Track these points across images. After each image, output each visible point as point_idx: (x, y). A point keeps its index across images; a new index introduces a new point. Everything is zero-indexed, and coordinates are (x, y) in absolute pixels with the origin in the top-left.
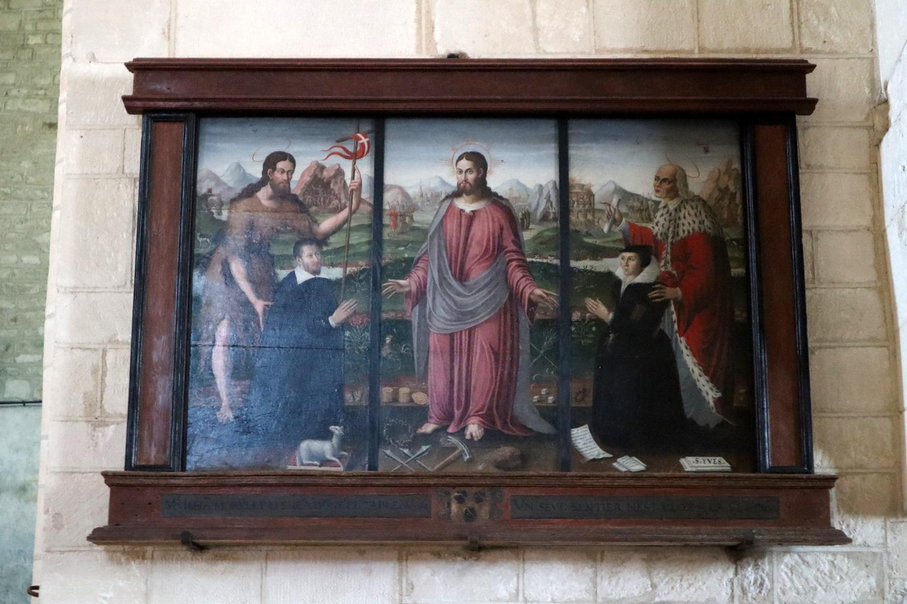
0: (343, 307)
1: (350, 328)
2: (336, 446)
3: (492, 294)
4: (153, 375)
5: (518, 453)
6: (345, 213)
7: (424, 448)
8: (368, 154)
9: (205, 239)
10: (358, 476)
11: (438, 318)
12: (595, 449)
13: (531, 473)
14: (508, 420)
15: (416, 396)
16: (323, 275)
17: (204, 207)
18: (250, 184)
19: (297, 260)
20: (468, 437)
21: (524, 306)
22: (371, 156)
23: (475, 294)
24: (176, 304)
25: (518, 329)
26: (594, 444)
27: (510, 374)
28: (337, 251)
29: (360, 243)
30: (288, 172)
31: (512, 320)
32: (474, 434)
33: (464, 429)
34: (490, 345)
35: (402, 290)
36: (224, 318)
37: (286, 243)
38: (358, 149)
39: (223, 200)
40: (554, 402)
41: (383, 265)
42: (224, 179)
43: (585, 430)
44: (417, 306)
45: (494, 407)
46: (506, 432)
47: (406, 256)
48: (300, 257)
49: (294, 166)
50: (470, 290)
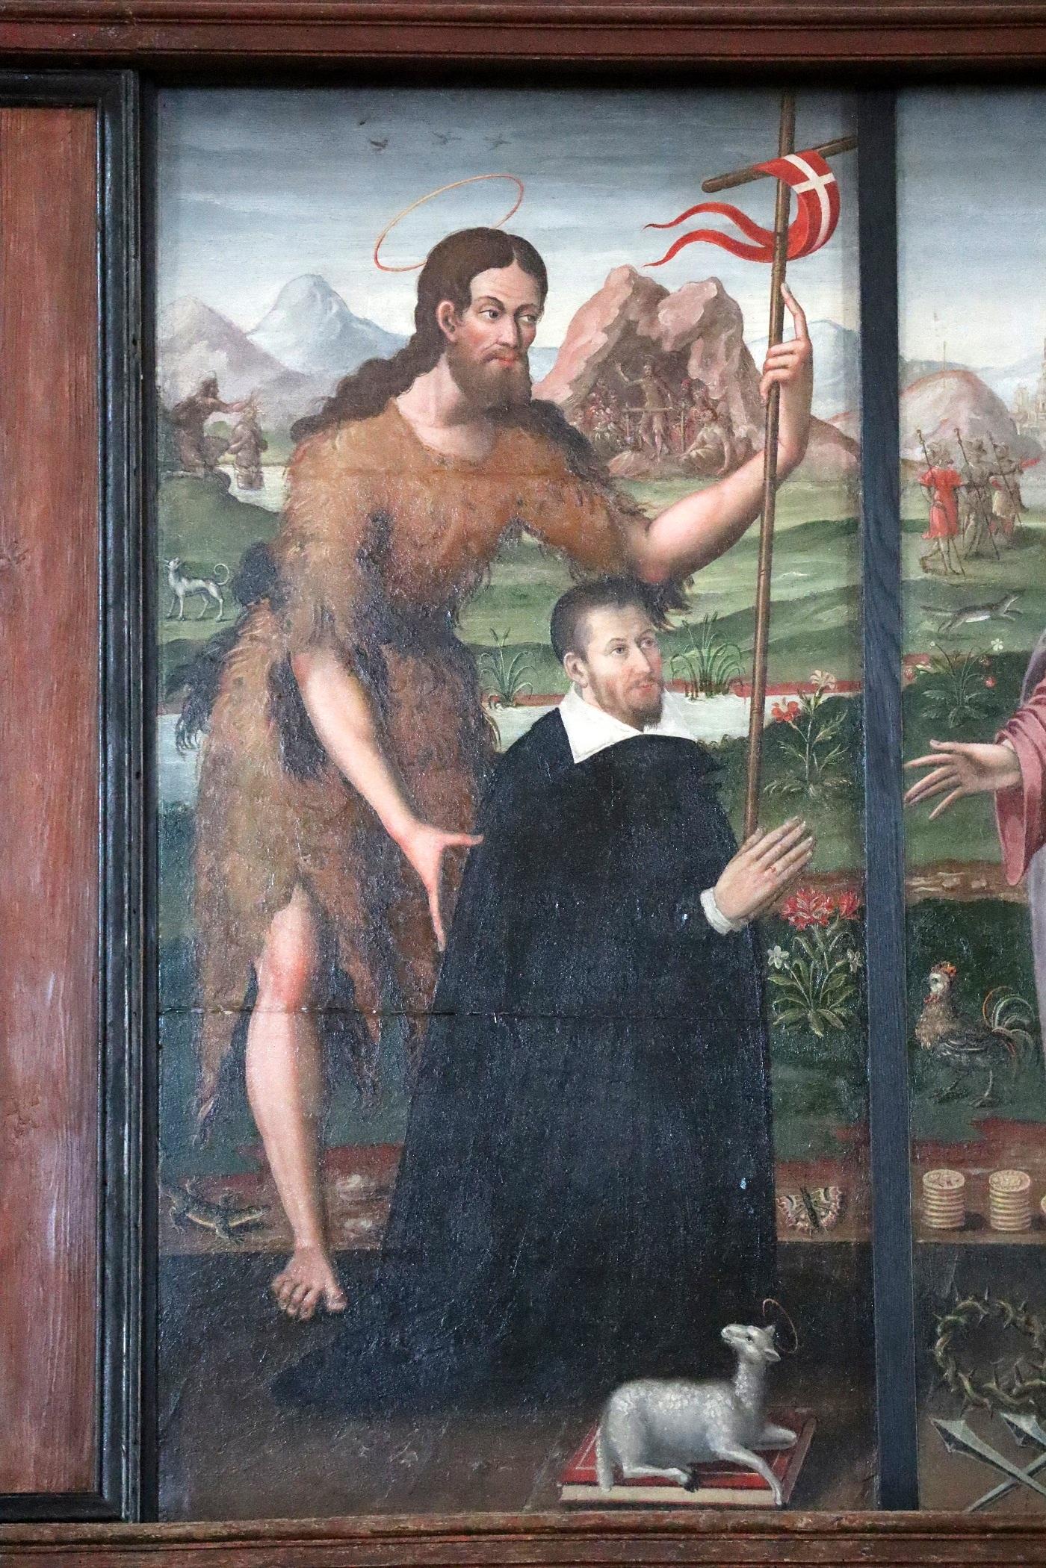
2: (749, 1404)
4: (19, 1132)
6: (750, 476)
8: (837, 235)
9: (200, 583)
10: (864, 1530)
16: (669, 727)
17: (191, 455)
18: (370, 364)
19: (569, 664)
22: (845, 245)
24: (99, 848)
28: (721, 629)
29: (814, 598)
30: (517, 314)
35: (986, 784)
36: (288, 898)
37: (521, 598)
38: (792, 219)
39: (263, 426)
41: (905, 683)
42: (262, 341)
47: (998, 646)
48: (583, 656)
49: (543, 289)
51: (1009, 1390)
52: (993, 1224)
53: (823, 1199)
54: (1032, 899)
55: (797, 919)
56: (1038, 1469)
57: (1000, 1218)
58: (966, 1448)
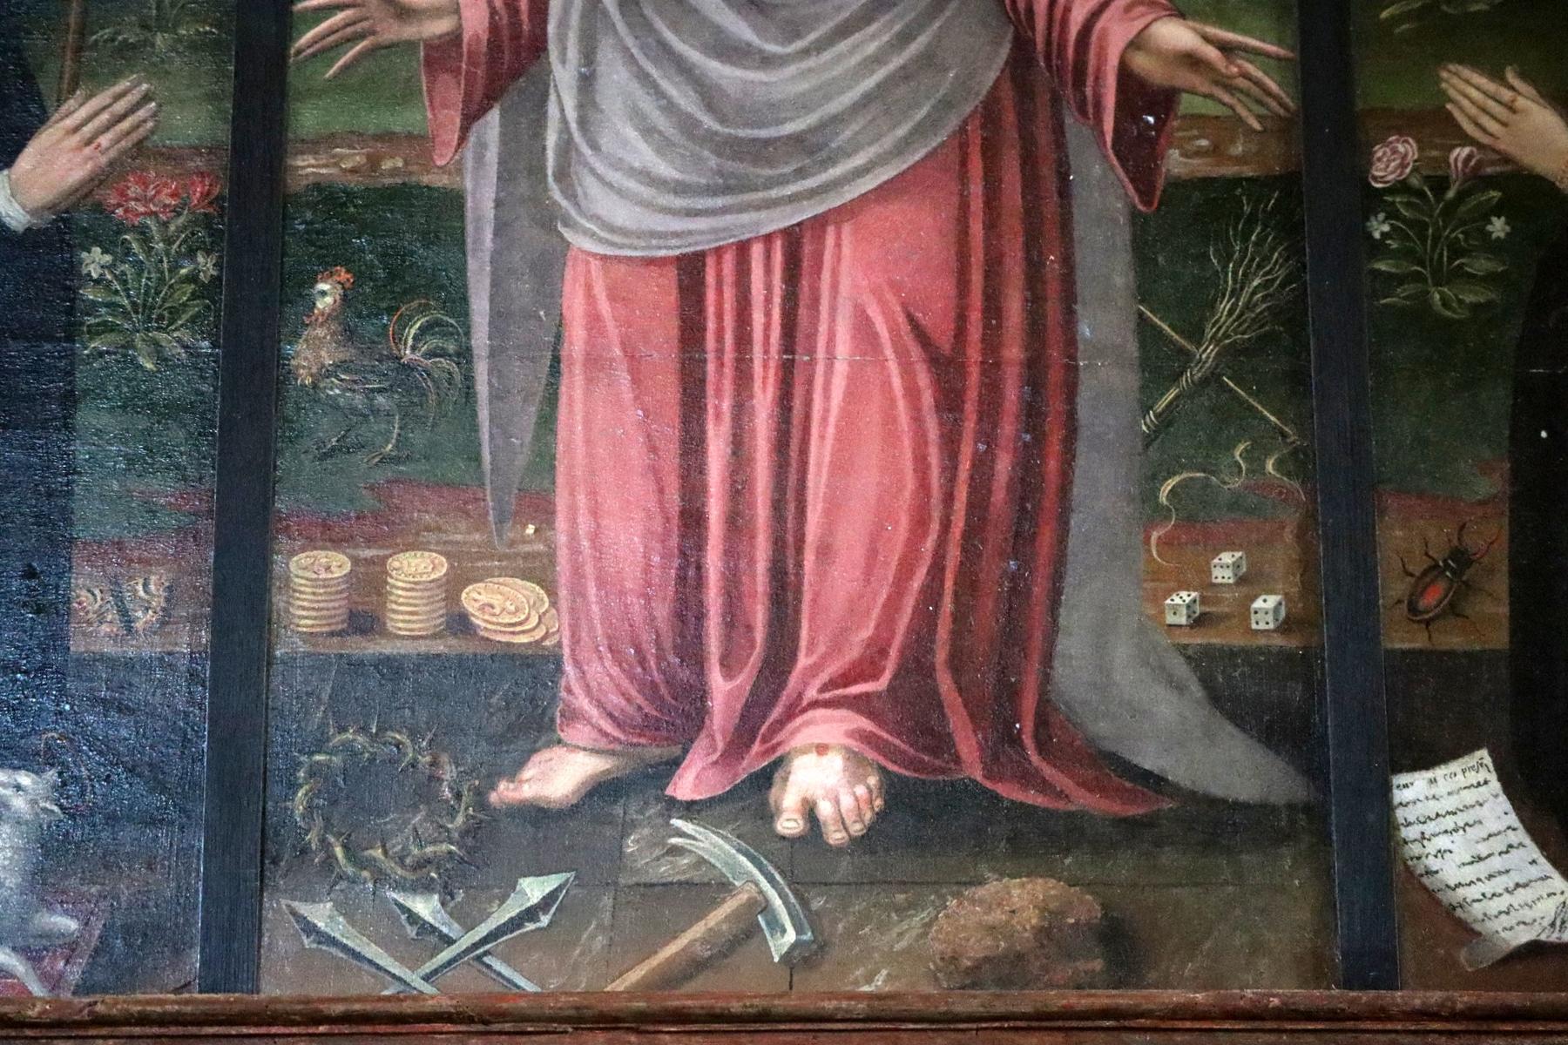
0: (69, 122)
1: (111, 240)
3: (921, 41)
5: (1086, 908)
7: (534, 889)
11: (615, 177)
12: (1541, 889)
13: (1175, 996)
14: (1026, 727)
15: (484, 598)
20: (789, 824)
21: (1098, 106)
23: (820, 46)
25: (1066, 224)
26: (1528, 859)
27: (1026, 485)
31: (1031, 182)
32: (825, 810)
33: (764, 780)
34: (911, 318)
35: (409, 31)
40: (1286, 627)
43: (1473, 778)
44: (494, 116)
45: (941, 655)
46: (1009, 792)
50: (793, 31)
51: (401, 861)
52: (389, 624)
53: (141, 593)
54: (469, 185)
55: (126, 211)
56: (436, 972)
57: (401, 617)
58: (334, 942)
